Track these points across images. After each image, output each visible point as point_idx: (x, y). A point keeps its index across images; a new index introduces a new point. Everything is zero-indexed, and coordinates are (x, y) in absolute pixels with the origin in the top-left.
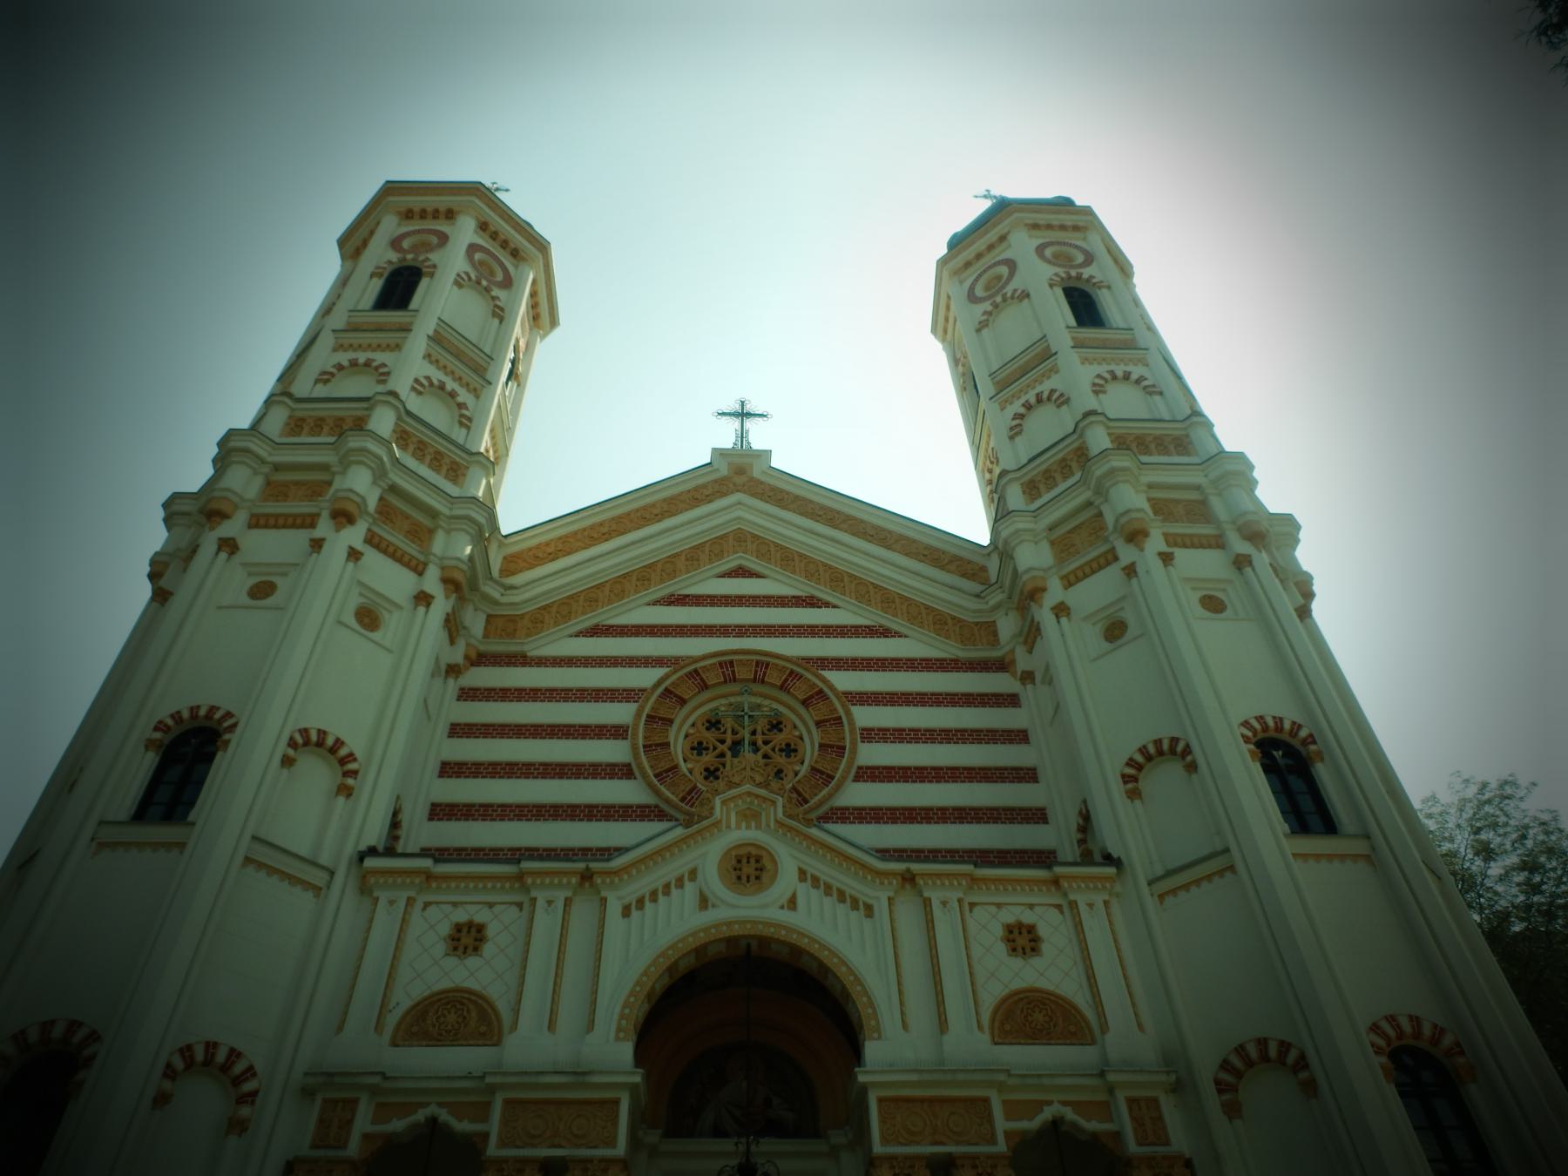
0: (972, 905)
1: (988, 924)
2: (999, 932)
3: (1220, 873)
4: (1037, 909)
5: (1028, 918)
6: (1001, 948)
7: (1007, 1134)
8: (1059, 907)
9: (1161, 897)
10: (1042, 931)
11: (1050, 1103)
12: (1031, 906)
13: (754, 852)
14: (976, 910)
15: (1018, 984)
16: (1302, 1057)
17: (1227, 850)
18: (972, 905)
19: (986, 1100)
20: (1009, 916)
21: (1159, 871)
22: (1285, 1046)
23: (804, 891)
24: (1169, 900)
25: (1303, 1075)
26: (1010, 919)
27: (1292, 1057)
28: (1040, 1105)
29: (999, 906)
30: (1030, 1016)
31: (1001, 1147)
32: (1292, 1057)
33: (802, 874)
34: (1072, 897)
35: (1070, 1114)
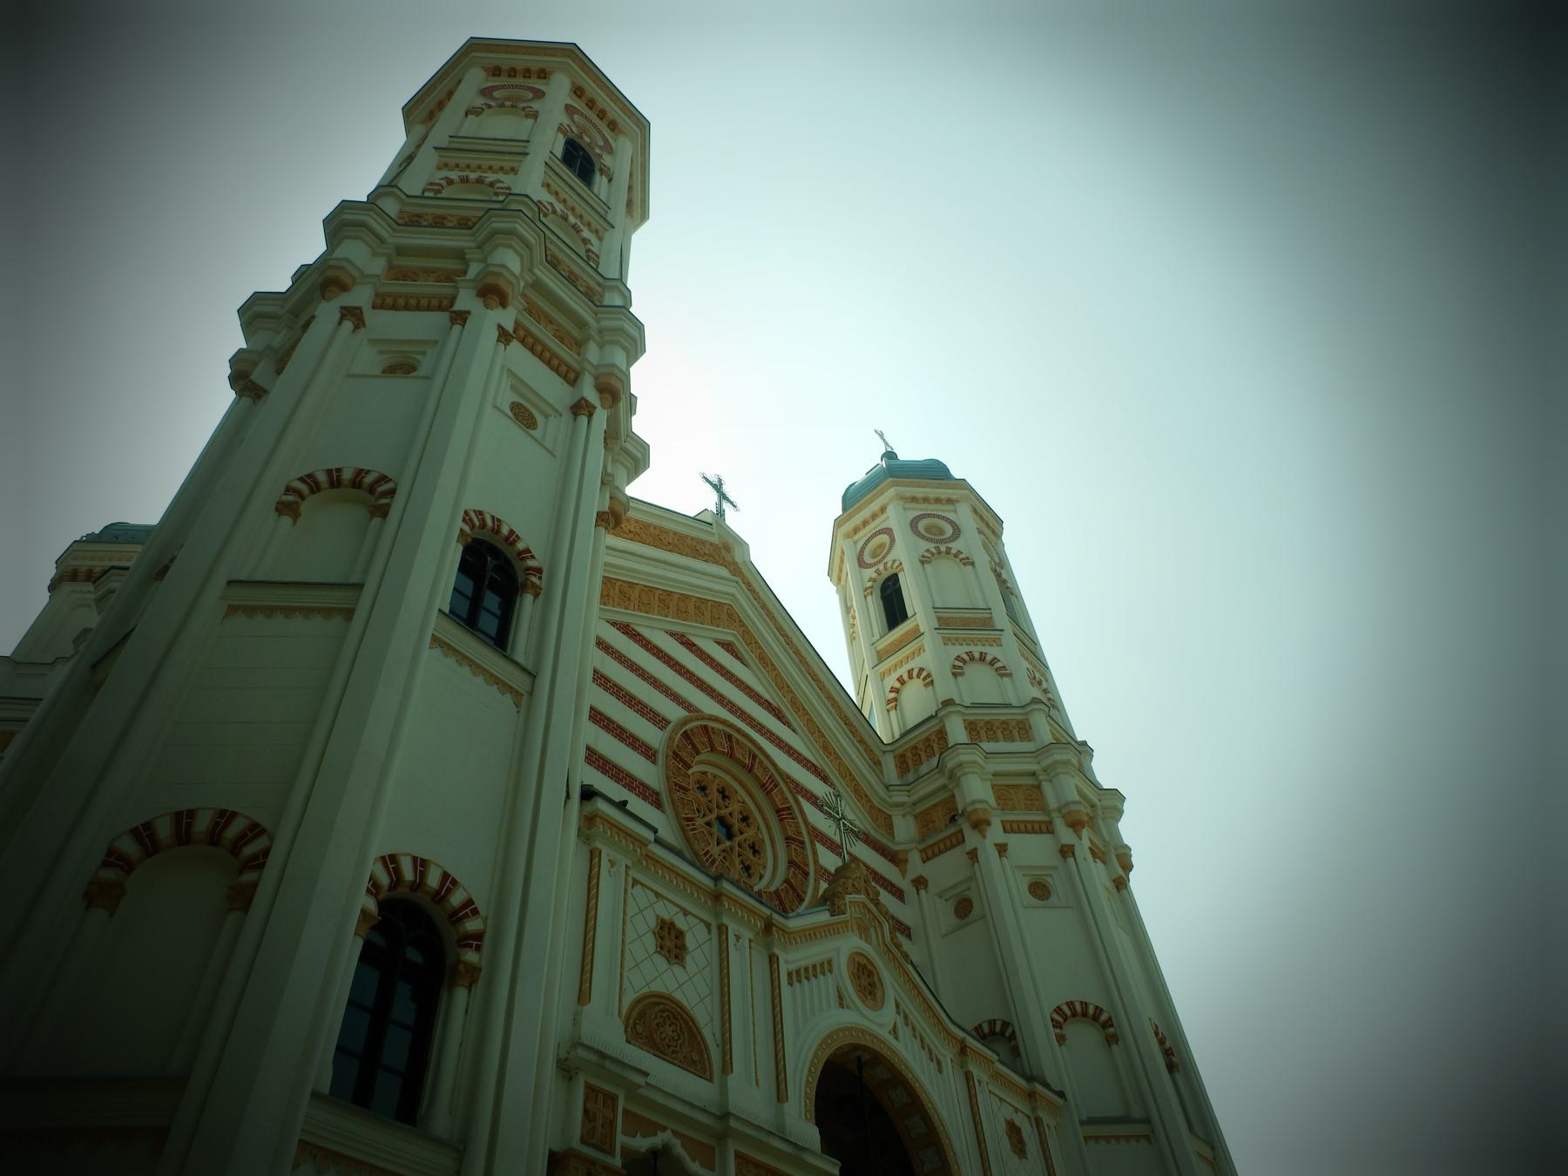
0: (635, 882)
1: (647, 909)
4: (690, 918)
5: (681, 923)
8: (708, 926)
10: (690, 942)
11: (664, 1129)
12: (686, 913)
15: (657, 987)
18: (635, 882)
20: (667, 912)
26: (666, 917)
28: (652, 1128)
29: (657, 895)
30: (659, 1023)
34: (725, 920)
35: (679, 1149)
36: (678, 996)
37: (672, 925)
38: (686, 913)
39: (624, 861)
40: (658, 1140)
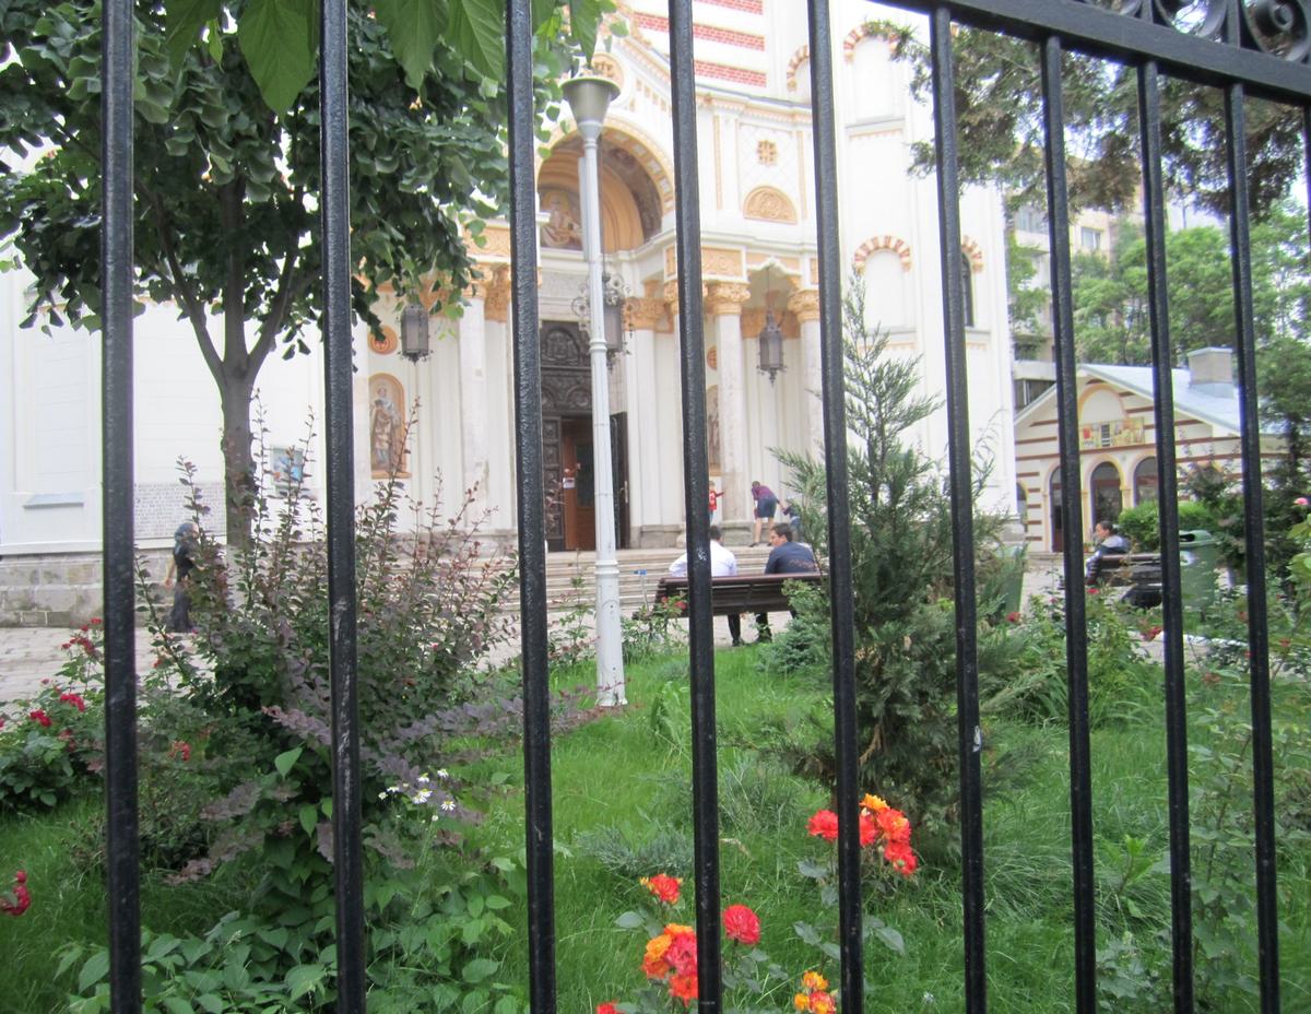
0: (741, 124)
1: (751, 138)
2: (756, 146)
3: (893, 131)
6: (755, 157)
7: (748, 271)
8: (790, 133)
9: (851, 137)
10: (779, 148)
12: (775, 130)
13: (608, 62)
14: (744, 127)
15: (761, 183)
16: (908, 250)
17: (903, 119)
19: (738, 252)
21: (853, 122)
22: (900, 243)
23: (640, 97)
24: (855, 140)
25: (905, 259)
27: (901, 249)
29: (757, 127)
31: (744, 279)
32: (901, 249)
33: (639, 83)
35: (778, 264)
36: (775, 184)
37: (766, 143)
38: (775, 130)
39: (733, 117)
40: (767, 263)
